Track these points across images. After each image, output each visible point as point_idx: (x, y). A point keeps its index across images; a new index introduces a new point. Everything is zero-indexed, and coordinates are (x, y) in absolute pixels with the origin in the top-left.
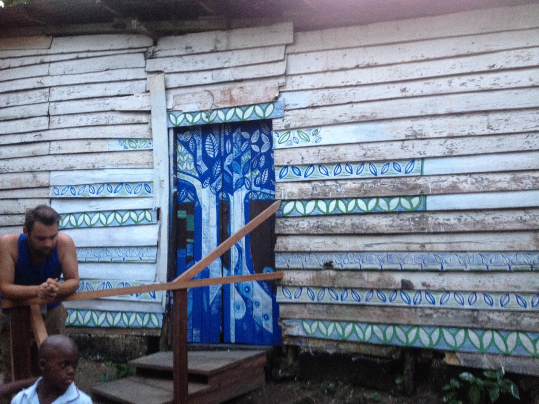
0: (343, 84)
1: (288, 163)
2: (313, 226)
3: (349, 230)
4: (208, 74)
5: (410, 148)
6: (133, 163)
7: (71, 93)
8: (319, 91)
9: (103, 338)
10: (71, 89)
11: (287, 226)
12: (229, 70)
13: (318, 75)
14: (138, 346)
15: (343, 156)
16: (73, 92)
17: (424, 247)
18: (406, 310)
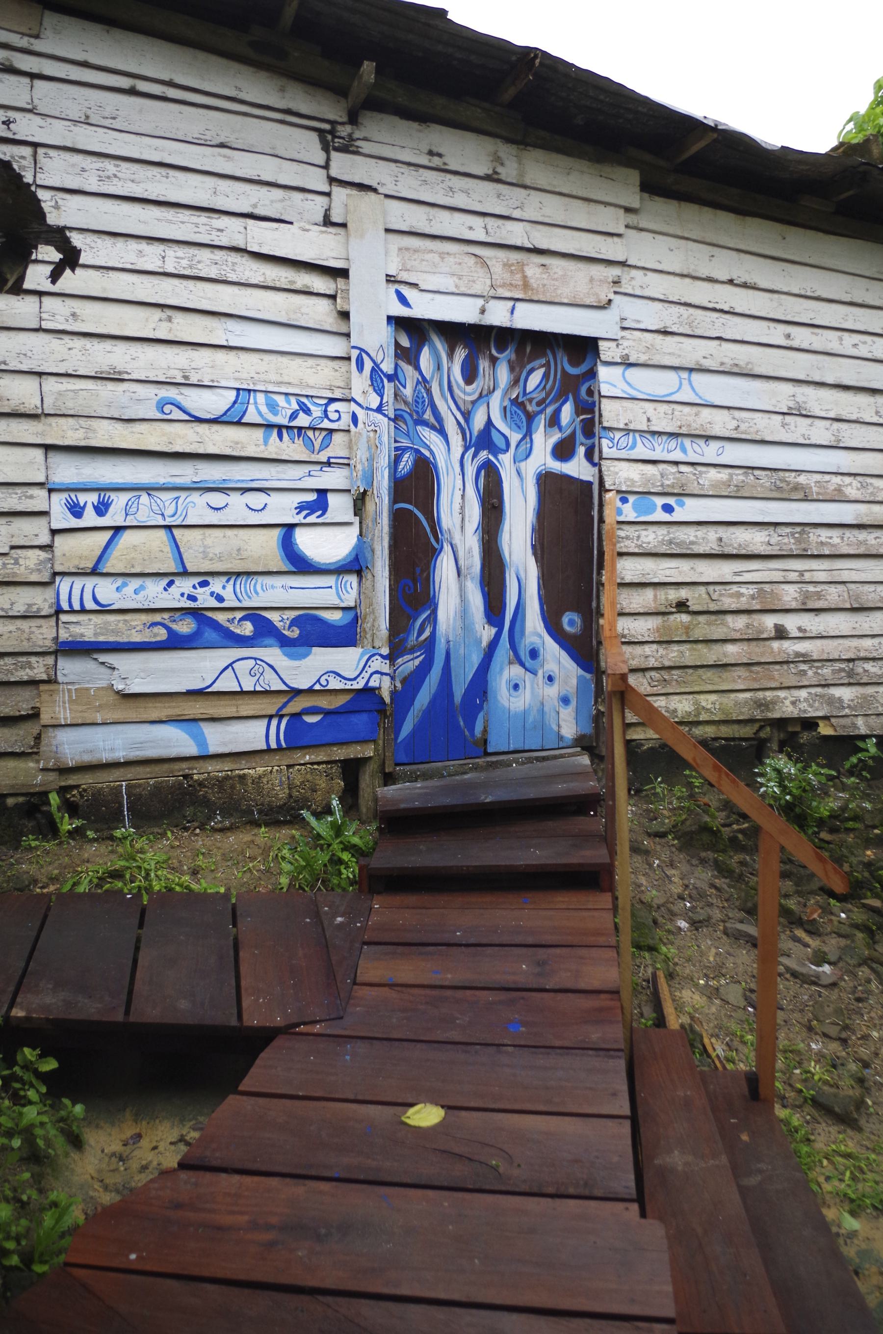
0: (710, 305)
1: (626, 424)
2: (663, 540)
3: (717, 550)
4: (477, 222)
5: (792, 427)
6: (291, 381)
7: (109, 177)
8: (672, 306)
9: (227, 778)
10: (110, 166)
11: (623, 538)
12: (521, 224)
13: (671, 277)
14: (322, 783)
15: (708, 425)
16: (115, 176)
17: (803, 575)
18: (777, 667)
